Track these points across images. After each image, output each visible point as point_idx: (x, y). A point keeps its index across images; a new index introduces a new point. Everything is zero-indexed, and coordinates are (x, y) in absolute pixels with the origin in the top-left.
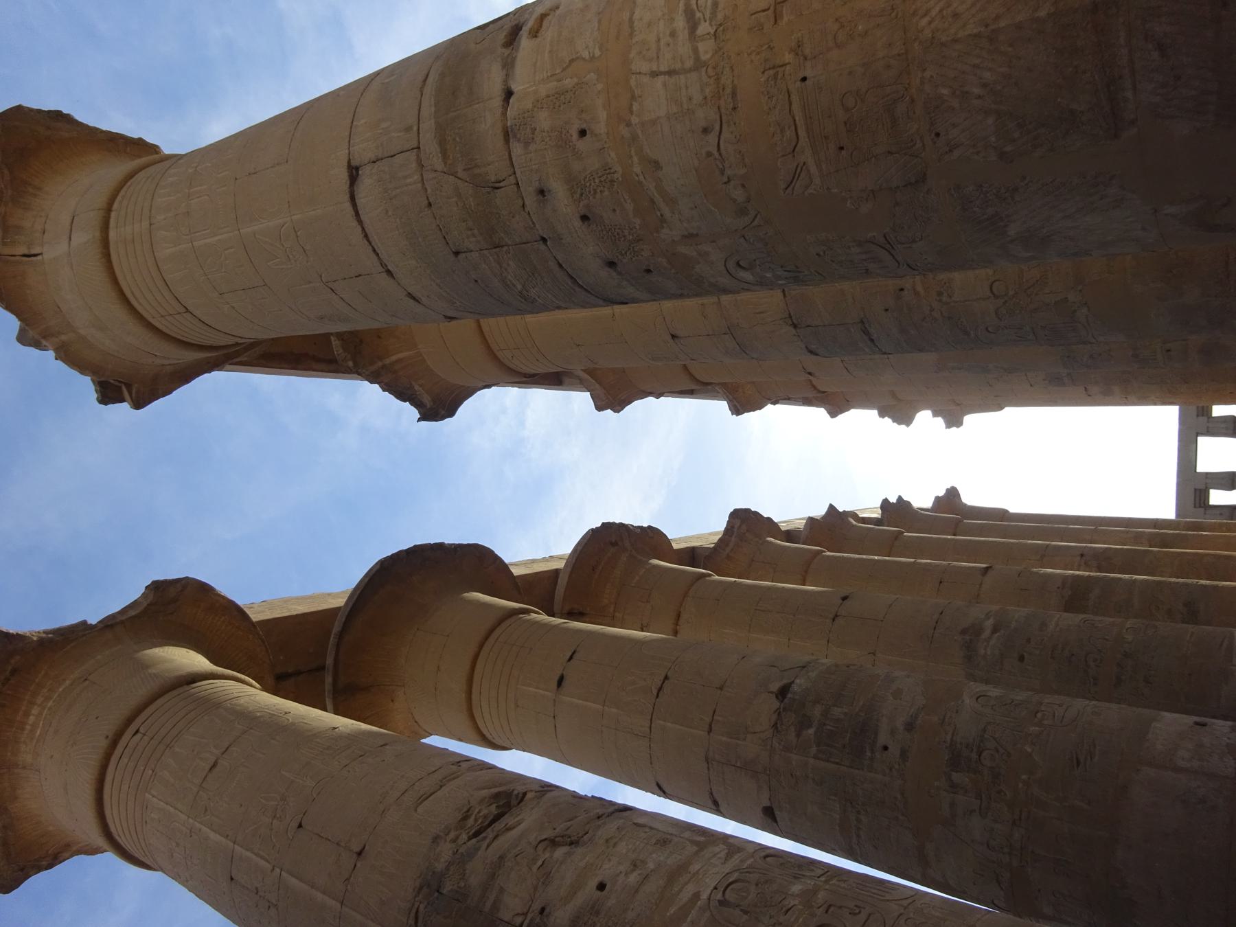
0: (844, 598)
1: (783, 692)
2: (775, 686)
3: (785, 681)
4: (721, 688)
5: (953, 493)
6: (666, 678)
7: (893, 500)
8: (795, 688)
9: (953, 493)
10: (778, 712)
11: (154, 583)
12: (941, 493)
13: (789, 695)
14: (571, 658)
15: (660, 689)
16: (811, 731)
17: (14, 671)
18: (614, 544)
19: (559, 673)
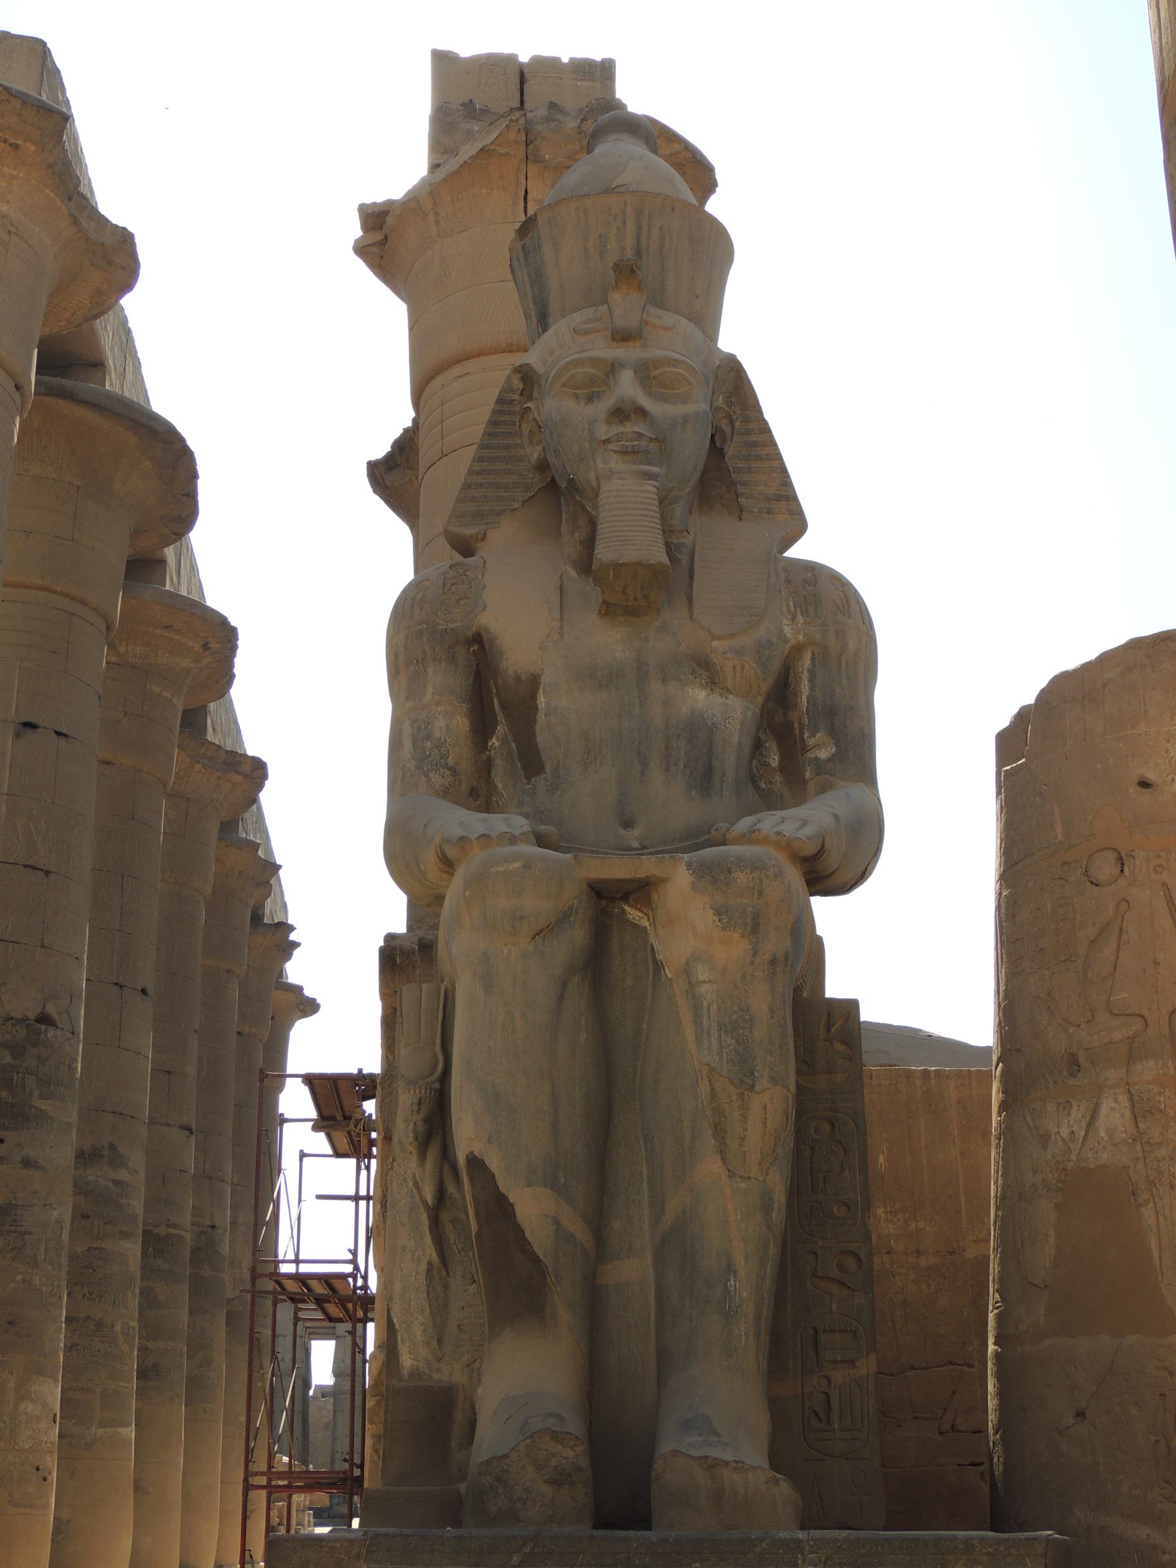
0: (144, 991)
1: (45, 1019)
2: (51, 1010)
3: (56, 1017)
4: (43, 946)
5: (309, 1007)
6: (47, 873)
7: (293, 937)
8: (51, 1032)
9: (309, 1007)
10: (25, 1019)
11: (131, 236)
12: (308, 992)
13: (43, 1027)
14: (58, 734)
15: (35, 868)
16: (8, 1059)
17: (16, 147)
18: (205, 647)
19: (40, 723)
